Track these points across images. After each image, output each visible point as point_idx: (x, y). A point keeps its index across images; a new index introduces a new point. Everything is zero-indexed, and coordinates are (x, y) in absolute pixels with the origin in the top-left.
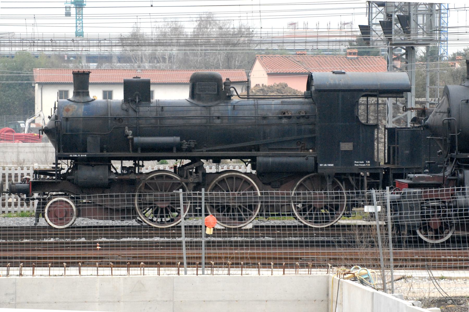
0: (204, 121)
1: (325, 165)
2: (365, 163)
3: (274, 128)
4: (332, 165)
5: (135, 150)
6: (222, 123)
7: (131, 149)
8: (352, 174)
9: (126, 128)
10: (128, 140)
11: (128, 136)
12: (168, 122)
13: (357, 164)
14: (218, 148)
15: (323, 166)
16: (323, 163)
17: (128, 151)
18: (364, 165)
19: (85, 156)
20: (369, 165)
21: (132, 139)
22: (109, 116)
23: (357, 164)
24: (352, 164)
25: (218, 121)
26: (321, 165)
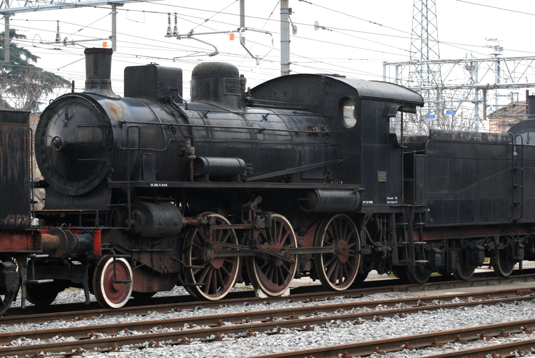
0: (248, 136)
1: (367, 202)
2: (394, 200)
3: (307, 148)
4: (371, 202)
5: (196, 179)
6: (264, 139)
7: (192, 176)
8: (382, 215)
9: (189, 142)
10: (190, 160)
11: (190, 154)
12: (219, 135)
13: (389, 200)
14: (266, 176)
15: (365, 204)
16: (366, 200)
17: (188, 180)
18: (393, 202)
19: (166, 185)
20: (397, 202)
21: (198, 161)
22: (161, 123)
23: (389, 200)
24: (385, 201)
25: (260, 136)
26: (364, 202)
